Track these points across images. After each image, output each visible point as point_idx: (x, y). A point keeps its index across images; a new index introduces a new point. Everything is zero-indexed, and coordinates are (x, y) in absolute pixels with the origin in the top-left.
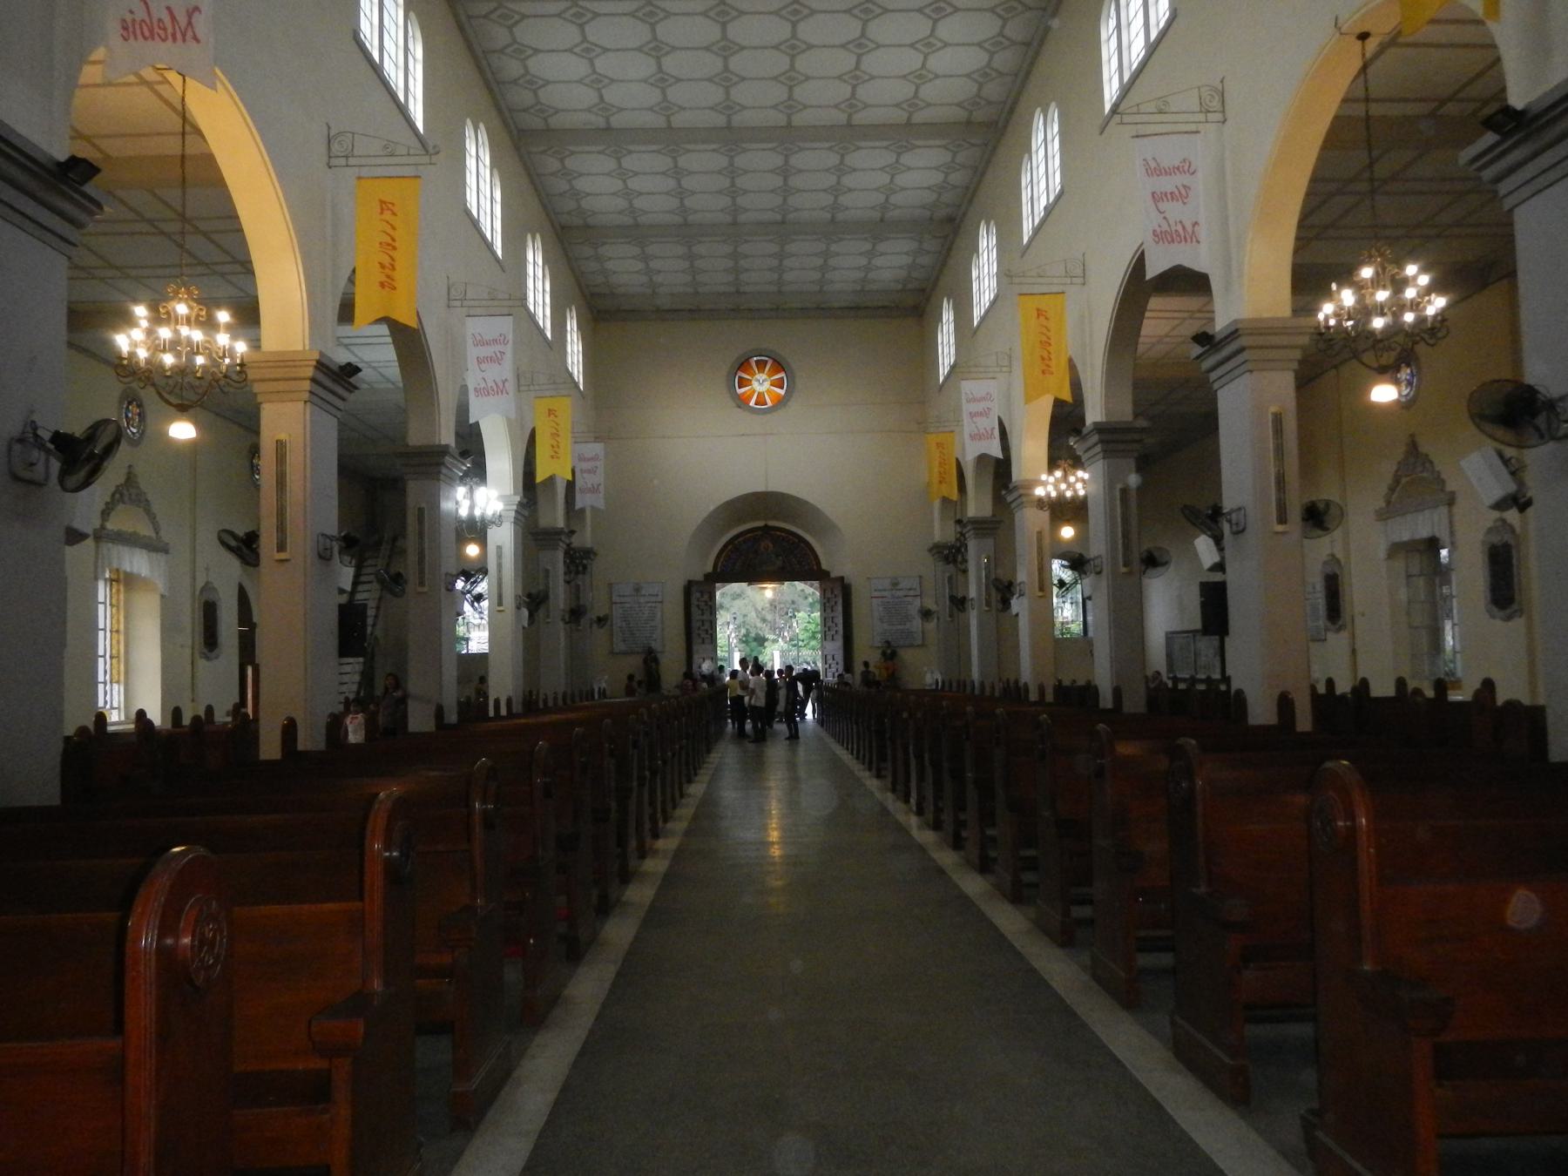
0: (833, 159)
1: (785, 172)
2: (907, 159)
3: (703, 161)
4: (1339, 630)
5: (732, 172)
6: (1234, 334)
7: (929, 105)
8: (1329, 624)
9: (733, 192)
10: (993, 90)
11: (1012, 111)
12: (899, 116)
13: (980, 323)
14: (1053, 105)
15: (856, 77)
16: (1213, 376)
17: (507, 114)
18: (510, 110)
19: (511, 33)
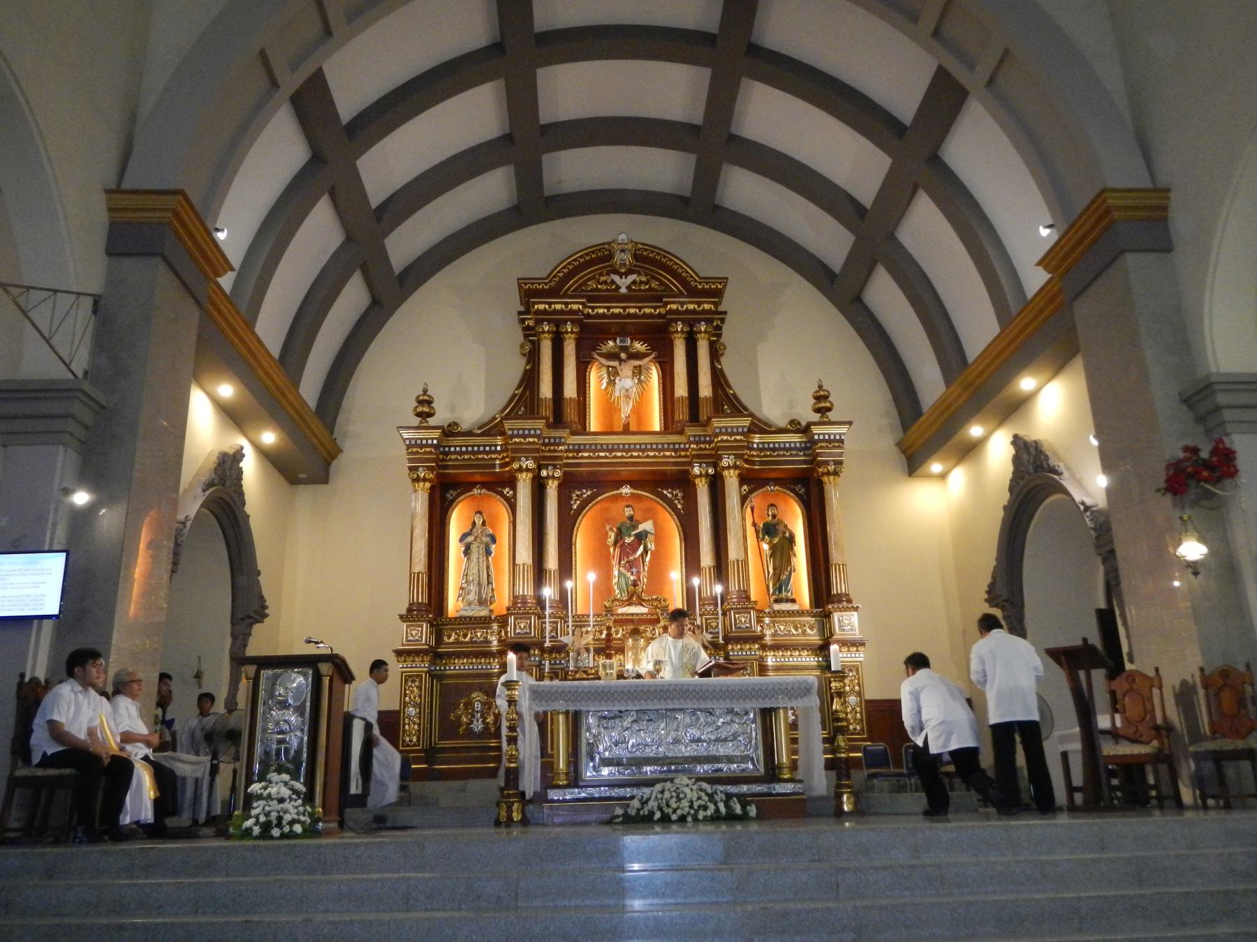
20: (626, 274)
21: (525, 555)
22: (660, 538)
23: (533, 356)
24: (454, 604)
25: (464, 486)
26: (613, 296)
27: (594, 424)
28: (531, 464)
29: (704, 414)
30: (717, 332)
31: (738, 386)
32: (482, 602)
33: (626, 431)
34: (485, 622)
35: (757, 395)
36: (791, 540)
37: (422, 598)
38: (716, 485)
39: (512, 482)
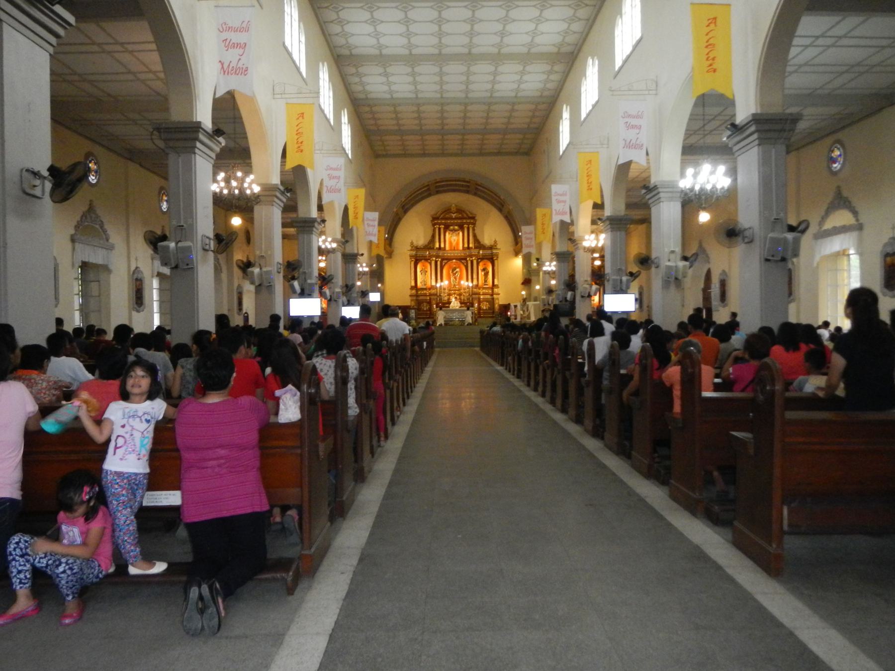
0: (492, 69)
1: (468, 74)
2: (528, 68)
3: (427, 71)
4: (724, 306)
5: (441, 74)
6: (655, 187)
7: (539, 45)
8: (720, 303)
9: (441, 83)
10: (571, 39)
11: (579, 50)
12: (524, 50)
13: (563, 154)
14: (596, 57)
15: (502, 34)
16: (650, 201)
17: (328, 36)
18: (329, 35)
19: (338, 15)
20: (454, 214)
21: (433, 277)
22: (461, 271)
23: (434, 230)
24: (419, 284)
25: (421, 260)
26: (451, 218)
27: (447, 248)
28: (434, 259)
29: (471, 245)
30: (474, 224)
31: (479, 237)
32: (425, 285)
33: (454, 250)
34: (425, 289)
35: (483, 237)
36: (488, 272)
37: (413, 284)
38: (472, 262)
39: (431, 261)
